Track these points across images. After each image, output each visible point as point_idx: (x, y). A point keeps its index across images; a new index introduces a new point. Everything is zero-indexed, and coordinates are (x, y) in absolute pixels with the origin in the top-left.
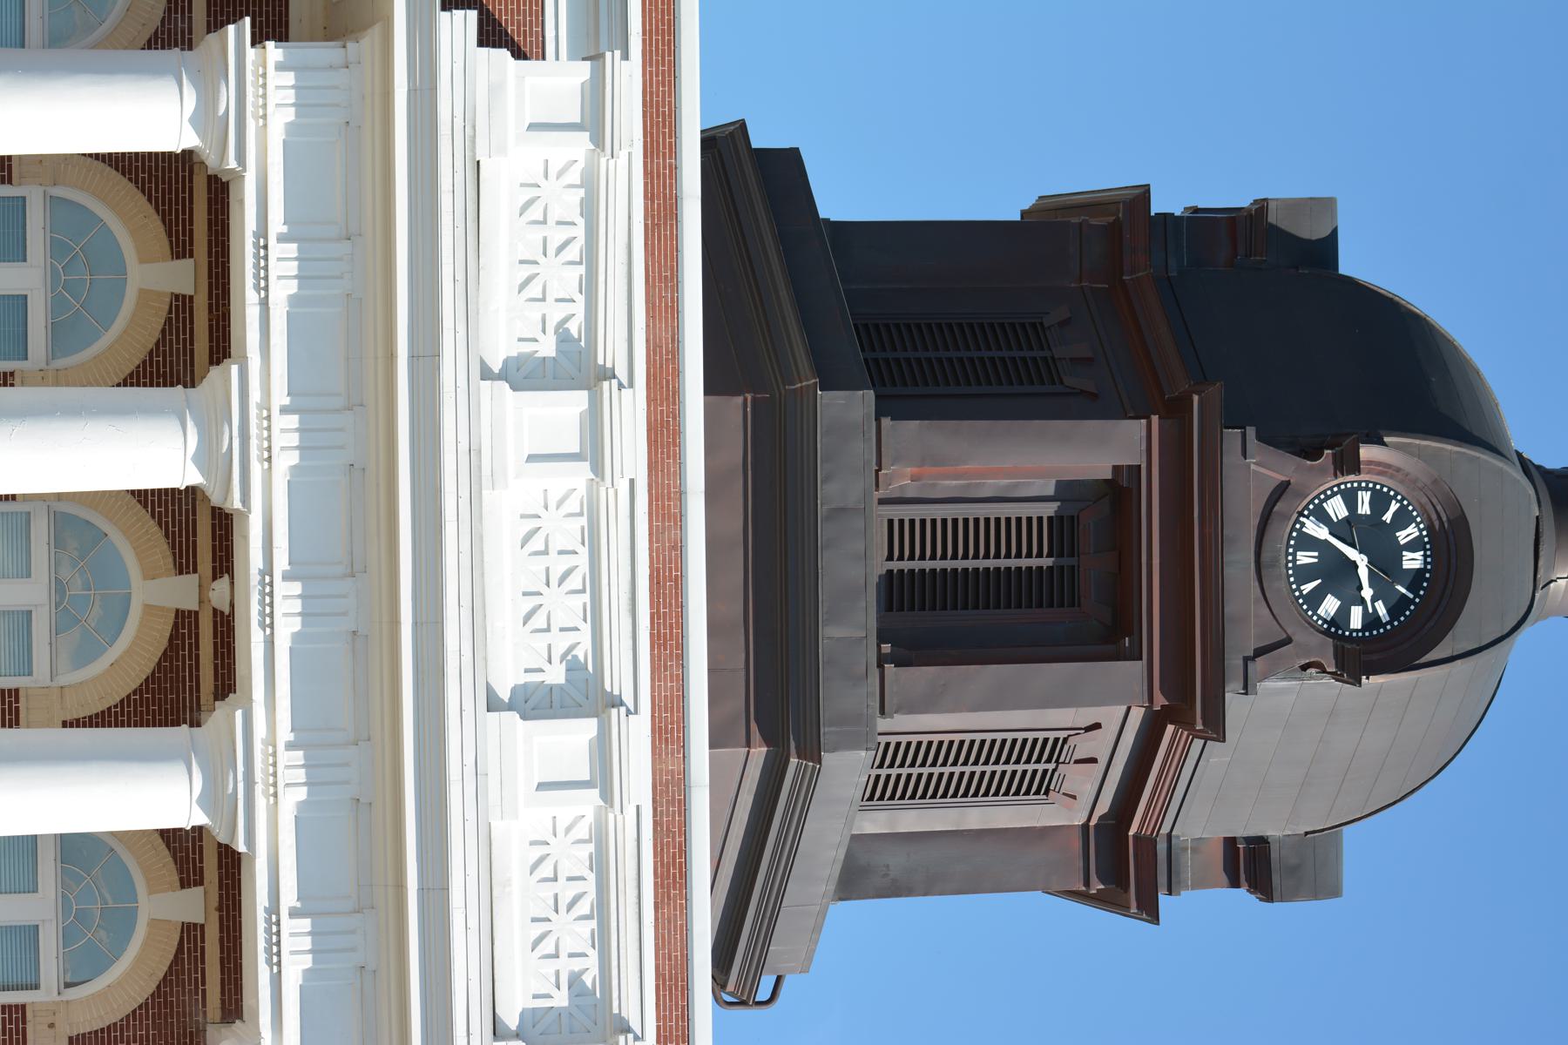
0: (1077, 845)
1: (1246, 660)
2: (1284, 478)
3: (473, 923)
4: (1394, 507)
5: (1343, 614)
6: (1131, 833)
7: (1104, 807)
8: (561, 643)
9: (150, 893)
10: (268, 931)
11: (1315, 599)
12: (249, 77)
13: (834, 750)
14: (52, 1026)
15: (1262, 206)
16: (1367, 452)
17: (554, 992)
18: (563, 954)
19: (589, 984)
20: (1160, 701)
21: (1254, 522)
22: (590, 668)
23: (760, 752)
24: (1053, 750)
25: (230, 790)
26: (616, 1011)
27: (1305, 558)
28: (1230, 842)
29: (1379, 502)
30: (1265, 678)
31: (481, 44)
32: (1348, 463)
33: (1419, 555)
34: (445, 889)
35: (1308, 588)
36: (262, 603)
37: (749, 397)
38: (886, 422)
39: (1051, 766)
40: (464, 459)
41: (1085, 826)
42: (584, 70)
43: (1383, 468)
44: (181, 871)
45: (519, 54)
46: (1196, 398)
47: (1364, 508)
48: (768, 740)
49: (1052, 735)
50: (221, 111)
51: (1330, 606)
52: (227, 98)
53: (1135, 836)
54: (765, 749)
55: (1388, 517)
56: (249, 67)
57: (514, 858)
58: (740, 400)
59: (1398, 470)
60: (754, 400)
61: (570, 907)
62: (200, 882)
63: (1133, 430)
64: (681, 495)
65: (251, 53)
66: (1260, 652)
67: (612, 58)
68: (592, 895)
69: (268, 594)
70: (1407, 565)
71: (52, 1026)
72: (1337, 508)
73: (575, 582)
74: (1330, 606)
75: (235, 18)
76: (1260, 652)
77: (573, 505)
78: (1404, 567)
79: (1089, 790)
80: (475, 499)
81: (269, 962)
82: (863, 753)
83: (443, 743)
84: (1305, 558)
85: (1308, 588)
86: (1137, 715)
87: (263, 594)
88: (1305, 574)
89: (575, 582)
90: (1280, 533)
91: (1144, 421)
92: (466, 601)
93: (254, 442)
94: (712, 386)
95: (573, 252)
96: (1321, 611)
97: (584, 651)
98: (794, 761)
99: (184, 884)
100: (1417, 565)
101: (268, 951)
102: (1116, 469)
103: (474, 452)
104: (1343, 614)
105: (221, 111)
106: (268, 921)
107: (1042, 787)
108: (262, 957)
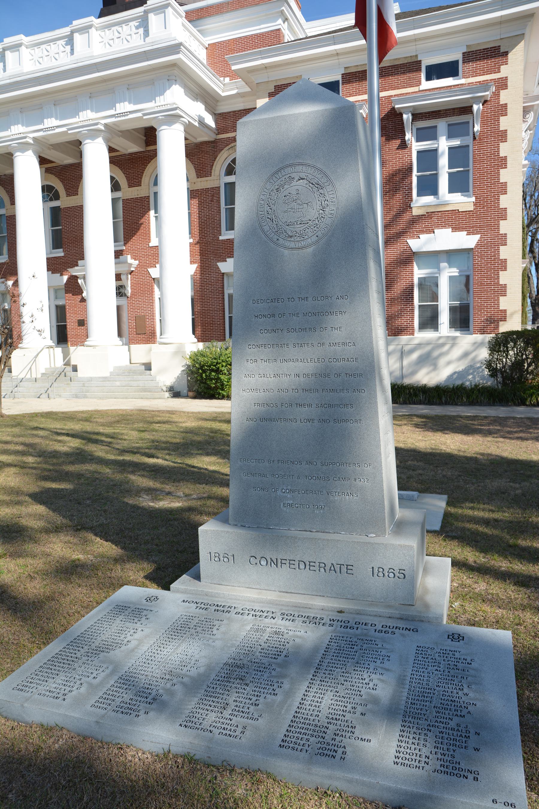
8: (62, 49)
10: (120, 116)
14: (195, 183)
17: (139, 34)
19: (138, 24)
22: (66, 39)
25: (86, 132)
34: (95, 64)
36: (50, 130)
61: (119, 33)
68: (116, 27)
69: (47, 129)
71: (195, 183)
73: (48, 48)
77: (32, 52)
81: (127, 115)
87: (48, 131)
89: (48, 48)
97: (62, 42)
101: (125, 116)
106: (118, 117)
108: (126, 118)
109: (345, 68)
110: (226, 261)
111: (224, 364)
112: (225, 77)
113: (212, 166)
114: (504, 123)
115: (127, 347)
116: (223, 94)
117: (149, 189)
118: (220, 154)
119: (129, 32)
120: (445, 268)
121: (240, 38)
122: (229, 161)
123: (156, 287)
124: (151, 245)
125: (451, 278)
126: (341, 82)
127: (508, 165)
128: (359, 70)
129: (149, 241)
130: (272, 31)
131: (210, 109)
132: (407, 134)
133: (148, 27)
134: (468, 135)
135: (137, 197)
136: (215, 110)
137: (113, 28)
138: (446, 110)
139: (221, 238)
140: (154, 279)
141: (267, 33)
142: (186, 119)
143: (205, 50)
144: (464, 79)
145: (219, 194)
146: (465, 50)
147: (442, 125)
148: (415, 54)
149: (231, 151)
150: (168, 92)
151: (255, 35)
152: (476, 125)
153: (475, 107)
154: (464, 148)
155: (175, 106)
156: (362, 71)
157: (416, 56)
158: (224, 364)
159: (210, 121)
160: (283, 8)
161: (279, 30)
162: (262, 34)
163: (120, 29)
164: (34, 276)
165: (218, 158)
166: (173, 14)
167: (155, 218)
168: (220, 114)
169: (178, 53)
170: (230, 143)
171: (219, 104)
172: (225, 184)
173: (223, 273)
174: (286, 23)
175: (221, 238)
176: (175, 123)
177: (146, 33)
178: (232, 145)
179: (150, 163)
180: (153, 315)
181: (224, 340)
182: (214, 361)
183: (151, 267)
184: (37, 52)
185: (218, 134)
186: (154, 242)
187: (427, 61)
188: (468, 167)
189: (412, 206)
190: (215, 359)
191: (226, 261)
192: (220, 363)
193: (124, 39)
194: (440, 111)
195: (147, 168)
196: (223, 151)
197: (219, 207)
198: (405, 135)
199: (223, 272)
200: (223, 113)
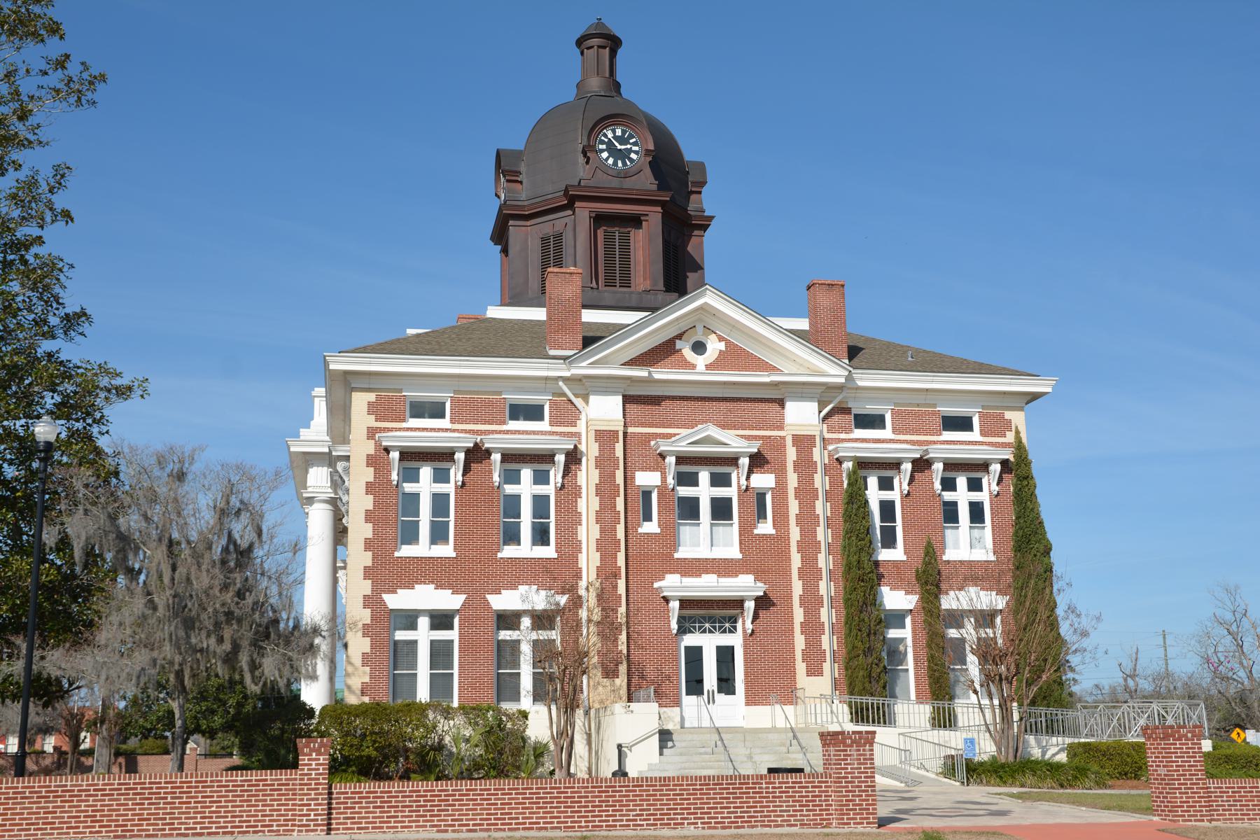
11: (631, 160)
27: (620, 164)
35: (628, 163)
47: (604, 147)
51: (633, 156)
72: (605, 155)
83: (969, 371)
84: (620, 164)
85: (628, 163)
88: (624, 164)
100: (620, 130)
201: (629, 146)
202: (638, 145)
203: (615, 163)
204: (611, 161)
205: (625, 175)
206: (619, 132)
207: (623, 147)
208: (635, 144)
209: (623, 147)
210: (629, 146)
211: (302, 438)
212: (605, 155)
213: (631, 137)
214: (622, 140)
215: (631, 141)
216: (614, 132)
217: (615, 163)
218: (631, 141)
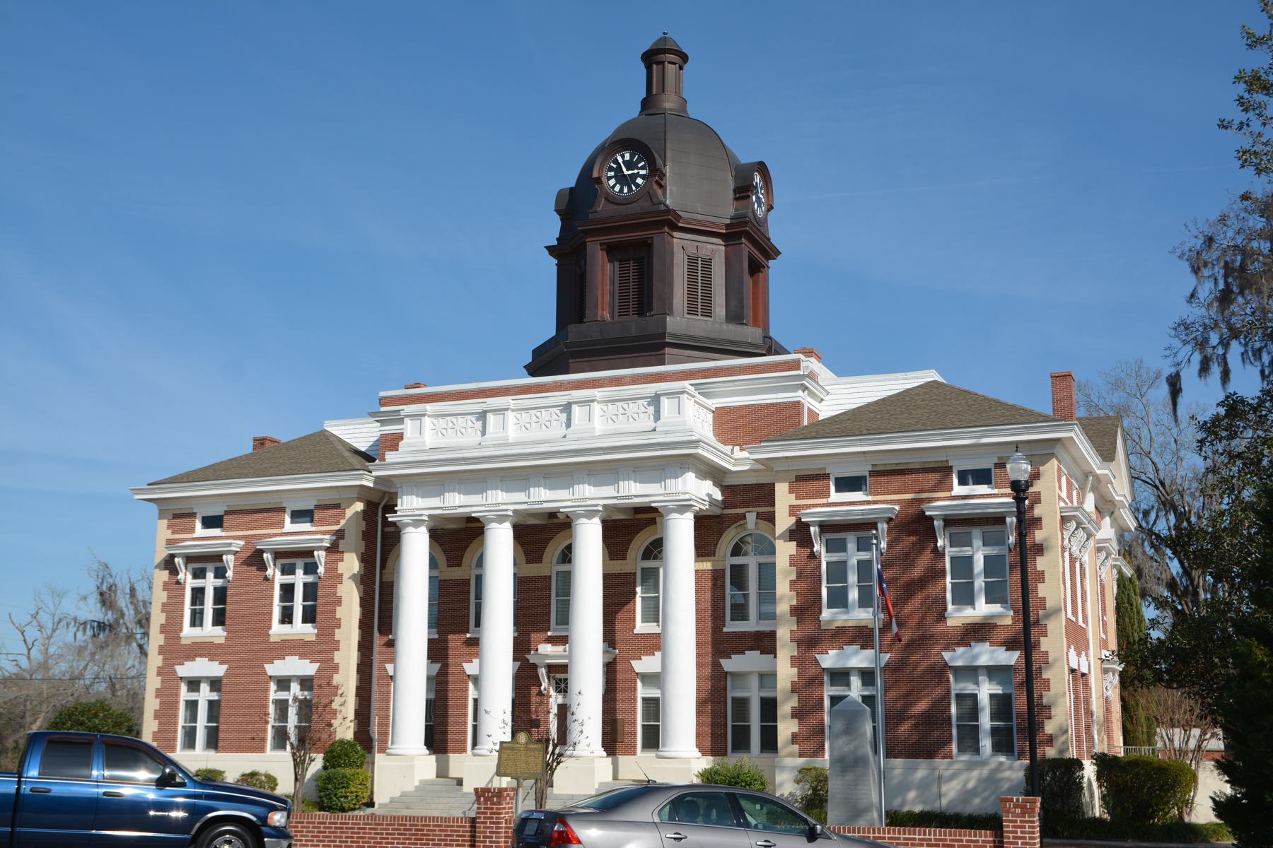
0: (730, 248)
1: (654, 205)
2: (603, 200)
3: (618, 439)
4: (612, 165)
5: (643, 177)
6: (724, 231)
7: (719, 241)
9: (657, 533)
11: (637, 185)
12: (405, 514)
13: (665, 328)
15: (556, 211)
16: (595, 175)
18: (637, 411)
20: (666, 229)
21: (616, 207)
23: (667, 350)
24: (692, 260)
26: (653, 395)
27: (626, 190)
28: (736, 199)
29: (611, 169)
30: (658, 199)
31: (397, 450)
32: (598, 181)
33: (626, 155)
35: (634, 188)
37: (570, 361)
38: (585, 320)
39: (700, 259)
40: (497, 449)
41: (725, 246)
42: (407, 420)
43: (601, 170)
44: (652, 524)
45: (402, 439)
46: (579, 228)
47: (612, 174)
48: (664, 348)
49: (686, 260)
50: (411, 522)
51: (639, 181)
52: (406, 520)
53: (726, 230)
54: (666, 349)
55: (615, 166)
56: (403, 514)
57: (611, 427)
58: (571, 364)
59: (601, 164)
60: (571, 359)
62: (655, 519)
63: (590, 246)
64: (556, 383)
65: (399, 513)
66: (652, 202)
67: (402, 413)
70: (628, 159)
73: (539, 414)
74: (639, 181)
75: (387, 518)
76: (652, 202)
77: (519, 416)
78: (628, 159)
79: (709, 246)
80: (512, 444)
81: (632, 499)
82: (668, 319)
84: (626, 190)
85: (634, 188)
86: (676, 234)
88: (630, 189)
89: (539, 414)
90: (625, 198)
91: (588, 243)
92: (532, 446)
93: (492, 509)
94: (567, 373)
95: (454, 420)
96: (640, 183)
97: (557, 410)
98: (667, 340)
99: (655, 523)
100: (628, 154)
102: (602, 250)
103: (494, 446)
104: (643, 177)
105: (411, 522)
107: (708, 262)
109: (873, 465)
110: (730, 658)
111: (743, 784)
112: (734, 445)
113: (717, 544)
114: (1039, 536)
115: (610, 759)
116: (733, 469)
117: (636, 564)
118: (726, 532)
119: (636, 410)
120: (984, 681)
121: (753, 405)
122: (737, 540)
123: (639, 684)
124: (635, 632)
125: (992, 696)
126: (868, 477)
127: (1046, 580)
128: (887, 469)
129: (634, 627)
130: (790, 402)
131: (718, 483)
132: (939, 540)
133: (659, 407)
134: (1005, 545)
135: (620, 572)
136: (722, 482)
137: (618, 403)
138: (980, 519)
139: (725, 630)
140: (637, 673)
141: (783, 403)
142: (698, 506)
143: (712, 414)
144: (996, 490)
145: (724, 577)
146: (997, 462)
147: (977, 535)
148: (945, 459)
149: (739, 530)
150: (680, 479)
151: (771, 404)
152: (1010, 537)
153: (1008, 520)
154: (1000, 558)
155: (687, 497)
156: (891, 470)
157: (947, 461)
158: (743, 784)
159: (718, 495)
160: (804, 382)
161: (799, 402)
162: (779, 404)
163: (625, 406)
164: (580, 693)
165: (724, 536)
166: (688, 398)
167: (640, 599)
168: (727, 486)
169: (697, 447)
170: (739, 521)
171: (727, 476)
172: (731, 565)
173: (727, 672)
174: (806, 392)
175: (725, 630)
176: (686, 512)
177: (657, 417)
178: (741, 522)
179: (639, 534)
180: (635, 719)
181: (725, 754)
182: (733, 780)
183: (635, 659)
184: (525, 416)
185: (725, 508)
186: (641, 627)
187: (959, 465)
188: (1005, 577)
189: (946, 615)
190: (734, 778)
191: (730, 658)
192: (738, 783)
193: (630, 417)
194: (973, 519)
195: (635, 539)
196: (729, 530)
197: (724, 593)
198: (937, 542)
199: (726, 671)
200: (731, 486)
201: (636, 171)
202: (645, 169)
203: (621, 190)
204: (617, 188)
205: (627, 202)
206: (627, 157)
207: (630, 172)
208: (642, 168)
209: (630, 172)
210: (636, 171)
211: (387, 460)
212: (612, 182)
213: (639, 161)
214: (630, 165)
215: (639, 165)
216: (623, 157)
217: (621, 190)
218: (639, 165)
